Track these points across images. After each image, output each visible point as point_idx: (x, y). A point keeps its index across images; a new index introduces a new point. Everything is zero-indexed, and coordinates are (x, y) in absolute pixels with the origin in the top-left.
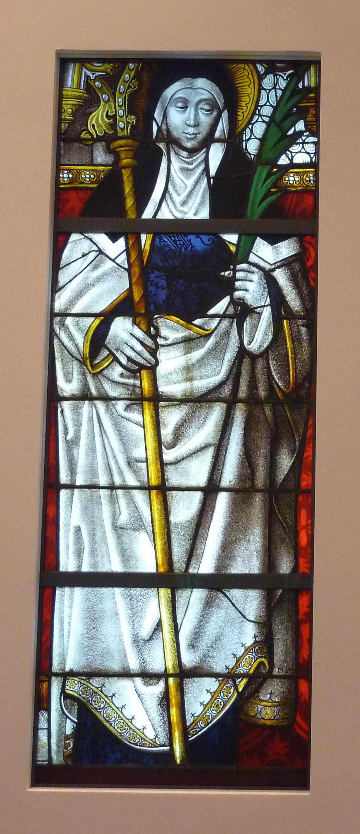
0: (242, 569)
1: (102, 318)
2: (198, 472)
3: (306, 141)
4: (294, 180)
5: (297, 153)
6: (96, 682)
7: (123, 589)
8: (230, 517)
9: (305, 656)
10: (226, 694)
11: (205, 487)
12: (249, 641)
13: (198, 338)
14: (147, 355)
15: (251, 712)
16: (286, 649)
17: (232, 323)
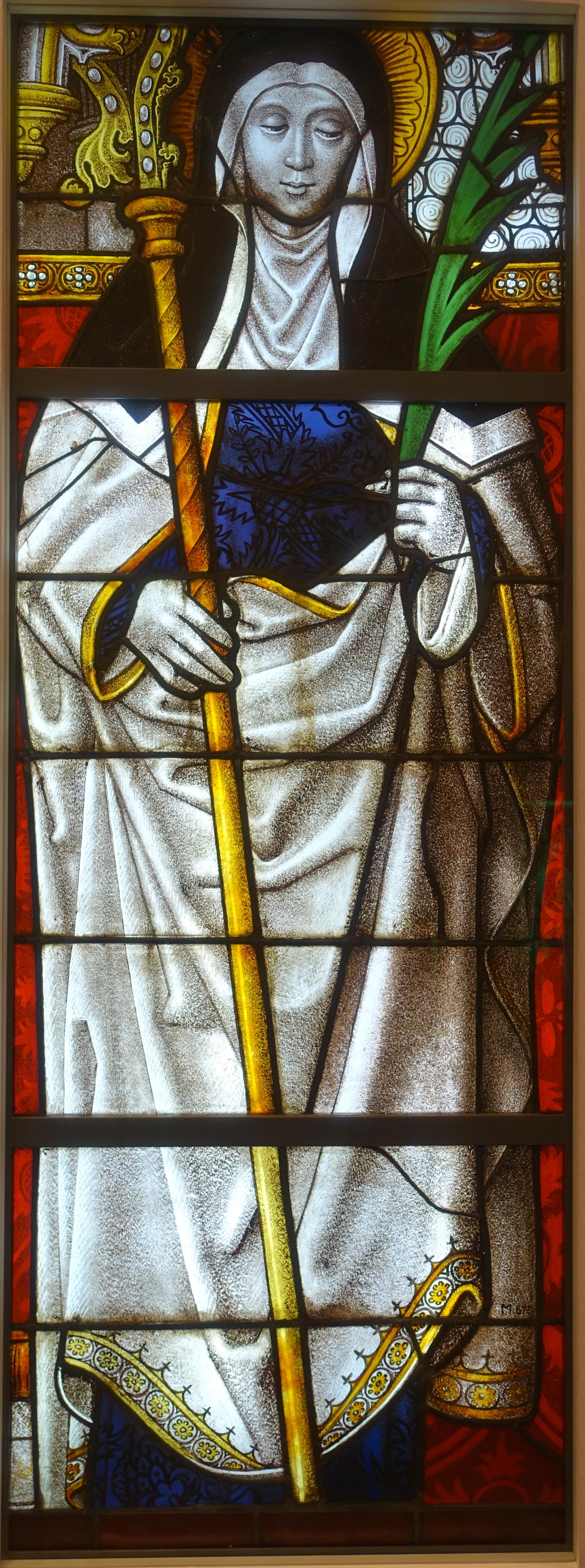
0: (424, 1105)
1: (119, 583)
2: (328, 906)
3: (540, 202)
4: (517, 285)
5: (521, 227)
6: (129, 1341)
7: (178, 1149)
8: (397, 998)
9: (557, 1280)
10: (395, 1359)
11: (344, 937)
12: (441, 1250)
13: (321, 625)
14: (217, 663)
15: (447, 1394)
16: (517, 1266)
17: (392, 592)
